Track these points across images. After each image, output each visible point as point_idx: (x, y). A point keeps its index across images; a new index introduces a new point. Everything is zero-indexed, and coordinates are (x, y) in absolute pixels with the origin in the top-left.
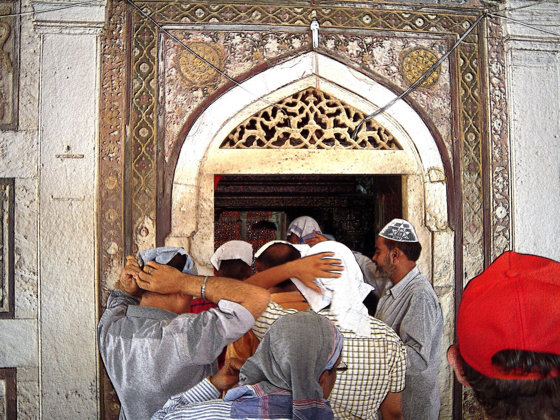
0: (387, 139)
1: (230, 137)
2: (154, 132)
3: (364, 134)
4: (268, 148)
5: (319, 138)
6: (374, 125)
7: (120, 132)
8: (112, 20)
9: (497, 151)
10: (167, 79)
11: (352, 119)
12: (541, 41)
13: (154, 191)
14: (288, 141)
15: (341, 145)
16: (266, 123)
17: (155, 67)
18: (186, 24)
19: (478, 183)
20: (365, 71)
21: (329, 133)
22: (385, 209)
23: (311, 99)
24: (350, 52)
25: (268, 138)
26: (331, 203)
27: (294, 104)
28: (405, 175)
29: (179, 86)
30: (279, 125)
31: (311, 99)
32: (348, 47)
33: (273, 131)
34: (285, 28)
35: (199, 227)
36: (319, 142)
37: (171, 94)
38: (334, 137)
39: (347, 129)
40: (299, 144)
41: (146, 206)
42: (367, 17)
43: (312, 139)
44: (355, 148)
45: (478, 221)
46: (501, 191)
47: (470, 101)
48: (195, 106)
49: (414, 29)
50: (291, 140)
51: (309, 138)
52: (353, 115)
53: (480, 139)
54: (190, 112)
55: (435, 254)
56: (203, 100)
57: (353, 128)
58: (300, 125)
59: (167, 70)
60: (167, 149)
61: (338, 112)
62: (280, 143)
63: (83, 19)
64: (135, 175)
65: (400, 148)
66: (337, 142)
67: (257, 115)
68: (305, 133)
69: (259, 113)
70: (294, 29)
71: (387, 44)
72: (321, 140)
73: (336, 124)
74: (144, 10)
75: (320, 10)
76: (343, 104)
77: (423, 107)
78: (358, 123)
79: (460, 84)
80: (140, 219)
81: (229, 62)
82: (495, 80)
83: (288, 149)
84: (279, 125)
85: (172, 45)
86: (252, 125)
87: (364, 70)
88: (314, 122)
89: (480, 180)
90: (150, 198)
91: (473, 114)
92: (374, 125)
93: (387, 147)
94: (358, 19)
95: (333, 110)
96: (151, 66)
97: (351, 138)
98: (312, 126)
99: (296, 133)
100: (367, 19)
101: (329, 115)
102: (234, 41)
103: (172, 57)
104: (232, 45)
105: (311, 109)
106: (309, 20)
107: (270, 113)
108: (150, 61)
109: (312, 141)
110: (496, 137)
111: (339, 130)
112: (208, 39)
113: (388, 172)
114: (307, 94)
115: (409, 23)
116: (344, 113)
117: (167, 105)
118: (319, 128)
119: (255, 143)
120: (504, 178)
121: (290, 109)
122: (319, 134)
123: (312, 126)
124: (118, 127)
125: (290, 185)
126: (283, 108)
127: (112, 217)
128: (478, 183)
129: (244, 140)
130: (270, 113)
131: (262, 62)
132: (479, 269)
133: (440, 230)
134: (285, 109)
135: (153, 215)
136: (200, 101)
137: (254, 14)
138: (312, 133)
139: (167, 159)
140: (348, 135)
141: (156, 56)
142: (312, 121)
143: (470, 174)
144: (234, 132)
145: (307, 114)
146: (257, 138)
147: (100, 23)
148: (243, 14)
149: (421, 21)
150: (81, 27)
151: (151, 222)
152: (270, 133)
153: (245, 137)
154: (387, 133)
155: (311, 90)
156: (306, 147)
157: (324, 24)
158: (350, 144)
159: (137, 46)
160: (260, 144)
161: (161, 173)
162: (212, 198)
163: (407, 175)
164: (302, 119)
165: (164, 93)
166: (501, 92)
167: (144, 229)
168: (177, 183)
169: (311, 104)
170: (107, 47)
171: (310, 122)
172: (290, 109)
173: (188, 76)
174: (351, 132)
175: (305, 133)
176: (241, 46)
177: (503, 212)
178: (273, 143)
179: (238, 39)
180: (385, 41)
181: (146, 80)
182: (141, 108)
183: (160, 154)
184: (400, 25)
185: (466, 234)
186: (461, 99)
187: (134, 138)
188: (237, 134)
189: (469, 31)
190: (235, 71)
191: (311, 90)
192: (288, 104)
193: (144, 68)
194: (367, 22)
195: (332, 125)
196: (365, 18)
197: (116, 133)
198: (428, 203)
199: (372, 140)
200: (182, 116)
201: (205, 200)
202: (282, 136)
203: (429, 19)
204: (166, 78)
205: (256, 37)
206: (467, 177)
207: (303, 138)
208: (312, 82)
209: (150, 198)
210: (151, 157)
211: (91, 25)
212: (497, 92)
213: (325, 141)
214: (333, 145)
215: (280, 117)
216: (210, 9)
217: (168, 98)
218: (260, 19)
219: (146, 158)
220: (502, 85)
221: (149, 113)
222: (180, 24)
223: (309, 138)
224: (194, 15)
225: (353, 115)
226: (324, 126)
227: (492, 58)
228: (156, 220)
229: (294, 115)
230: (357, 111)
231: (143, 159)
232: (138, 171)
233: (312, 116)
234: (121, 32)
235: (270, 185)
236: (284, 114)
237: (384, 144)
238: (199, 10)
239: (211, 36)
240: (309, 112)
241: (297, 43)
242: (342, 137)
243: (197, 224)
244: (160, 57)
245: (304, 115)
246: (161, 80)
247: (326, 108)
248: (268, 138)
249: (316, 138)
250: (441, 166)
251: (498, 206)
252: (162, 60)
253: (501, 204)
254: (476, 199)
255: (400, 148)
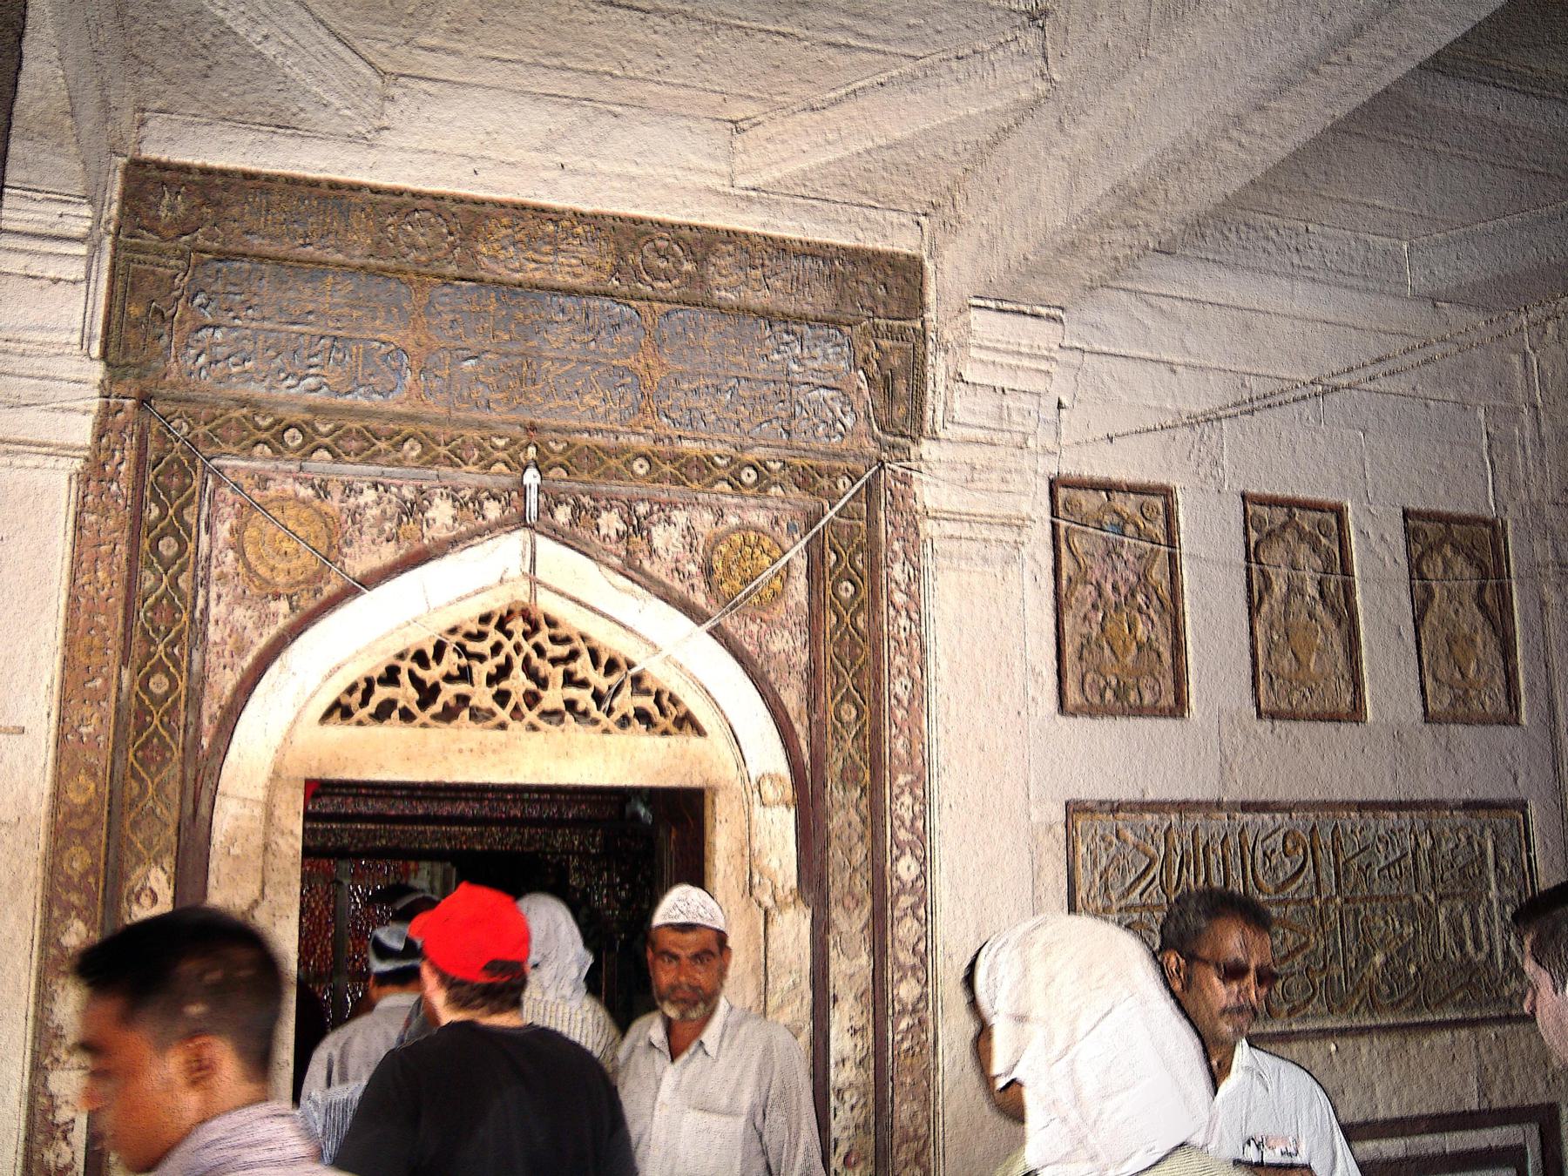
0: (675, 713)
1: (345, 700)
2: (182, 685)
3: (626, 702)
4: (424, 725)
5: (530, 708)
6: (647, 683)
7: (106, 680)
8: (104, 440)
9: (900, 742)
10: (214, 572)
11: (602, 670)
12: (989, 521)
13: (175, 814)
14: (465, 713)
15: (576, 725)
16: (420, 672)
17: (191, 546)
18: (261, 459)
19: (862, 807)
20: (632, 573)
21: (553, 697)
22: (676, 861)
23: (517, 625)
24: (603, 531)
25: (423, 704)
26: (563, 842)
27: (481, 636)
28: (711, 788)
29: (239, 590)
30: (449, 678)
31: (517, 625)
32: (599, 521)
33: (436, 689)
34: (469, 477)
35: (267, 890)
36: (531, 716)
37: (222, 605)
38: (562, 707)
39: (592, 690)
40: (487, 719)
41: (155, 840)
42: (641, 461)
43: (516, 708)
44: (606, 731)
45: (861, 886)
46: (908, 823)
47: (848, 637)
48: (271, 632)
49: (736, 484)
50: (471, 709)
51: (510, 707)
52: (604, 661)
53: (867, 716)
54: (261, 643)
55: (769, 955)
56: (288, 620)
57: (603, 687)
58: (491, 680)
59: (215, 552)
60: (206, 721)
61: (574, 655)
62: (448, 715)
63: (43, 437)
64: (135, 775)
65: (699, 731)
66: (568, 717)
67: (401, 656)
68: (502, 698)
69: (407, 651)
70: (488, 480)
71: (680, 517)
72: (536, 711)
73: (569, 679)
74: (176, 423)
75: (546, 444)
76: (584, 638)
77: (750, 648)
78: (614, 679)
79: (828, 602)
80: (139, 871)
81: (349, 543)
82: (899, 598)
83: (465, 731)
84: (449, 678)
85: (230, 502)
86: (391, 676)
87: (631, 569)
88: (523, 676)
89: (865, 801)
90: (166, 825)
91: (853, 664)
92: (647, 683)
93: (673, 729)
94: (622, 466)
95: (562, 651)
96: (183, 546)
97: (599, 708)
98: (518, 683)
99: (482, 696)
100: (641, 466)
101: (554, 661)
102: (362, 500)
103: (227, 525)
104: (358, 507)
105: (518, 648)
106: (520, 463)
107: (430, 653)
108: (182, 533)
109: (516, 713)
110: (900, 713)
111: (573, 693)
112: (306, 492)
113: (673, 782)
114: (510, 612)
115: (727, 475)
116: (585, 657)
117: (211, 628)
118: (532, 686)
119: (395, 714)
120: (915, 798)
121: (472, 647)
122: (532, 699)
123: (518, 683)
124: (104, 670)
125: (467, 800)
126: (457, 644)
127: (76, 865)
128: (862, 807)
129: (372, 707)
130: (430, 653)
131: (417, 546)
132: (864, 986)
133: (780, 906)
134: (461, 646)
135: (168, 862)
136: (282, 622)
137: (407, 446)
138: (516, 698)
139: (205, 742)
140: (593, 705)
141: (195, 521)
142: (518, 674)
143: (844, 789)
144: (351, 690)
145: (508, 659)
146: (400, 705)
147: (81, 449)
148: (382, 445)
149: (752, 472)
150: (38, 453)
151: (163, 878)
152: (428, 694)
153: (375, 701)
154: (673, 700)
155: (518, 609)
156: (502, 726)
157: (551, 474)
158: (596, 722)
159: (156, 498)
160: (407, 716)
161: (190, 773)
162: (299, 831)
163: (714, 791)
164: (498, 667)
165: (207, 602)
166: (911, 619)
167: (148, 892)
168: (224, 795)
169: (518, 637)
170: (90, 498)
171: (513, 673)
172: (472, 647)
173: (262, 570)
174: (598, 697)
175: (502, 698)
176: (376, 511)
177: (912, 868)
178: (435, 717)
179: (370, 496)
180: (676, 512)
181: (170, 572)
182: (156, 630)
183: (191, 731)
184: (707, 480)
185: (837, 914)
186: (828, 636)
187: (137, 695)
188: (358, 696)
189: (848, 496)
190: (361, 561)
191: (518, 609)
192: (469, 636)
193: (168, 547)
194: (642, 472)
195: (560, 680)
196: (636, 465)
197: (99, 682)
198: (756, 845)
199: (643, 716)
200: (240, 650)
201: (283, 833)
202: (452, 703)
203: (769, 470)
204: (212, 568)
205: (408, 493)
206: (838, 794)
207: (496, 708)
208: (521, 593)
209: (166, 825)
210: (172, 737)
211: (63, 450)
212: (903, 621)
213: (545, 714)
214: (562, 721)
215: (451, 662)
216: (315, 430)
217: (215, 611)
218: (419, 457)
219: (161, 738)
220: (913, 607)
221: (173, 644)
222: (250, 457)
223: (510, 707)
224: (282, 442)
225: (604, 660)
226: (543, 683)
227: (893, 551)
228: (176, 874)
229: (481, 658)
230: (612, 654)
231: (155, 740)
232: (142, 765)
233: (518, 662)
234: (123, 468)
235: (420, 799)
236: (460, 657)
237: (667, 723)
238: (292, 430)
239: (313, 486)
240: (513, 654)
241: (493, 510)
242: (581, 707)
243: (264, 884)
244: (202, 525)
245: (501, 659)
246: (201, 574)
247: (547, 645)
248: (423, 704)
249: (524, 708)
250: (782, 768)
251: (903, 853)
252: (207, 532)
253: (908, 850)
254: (856, 839)
255: (699, 731)
